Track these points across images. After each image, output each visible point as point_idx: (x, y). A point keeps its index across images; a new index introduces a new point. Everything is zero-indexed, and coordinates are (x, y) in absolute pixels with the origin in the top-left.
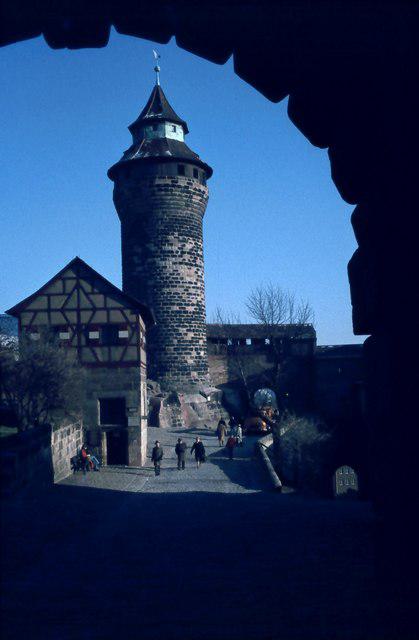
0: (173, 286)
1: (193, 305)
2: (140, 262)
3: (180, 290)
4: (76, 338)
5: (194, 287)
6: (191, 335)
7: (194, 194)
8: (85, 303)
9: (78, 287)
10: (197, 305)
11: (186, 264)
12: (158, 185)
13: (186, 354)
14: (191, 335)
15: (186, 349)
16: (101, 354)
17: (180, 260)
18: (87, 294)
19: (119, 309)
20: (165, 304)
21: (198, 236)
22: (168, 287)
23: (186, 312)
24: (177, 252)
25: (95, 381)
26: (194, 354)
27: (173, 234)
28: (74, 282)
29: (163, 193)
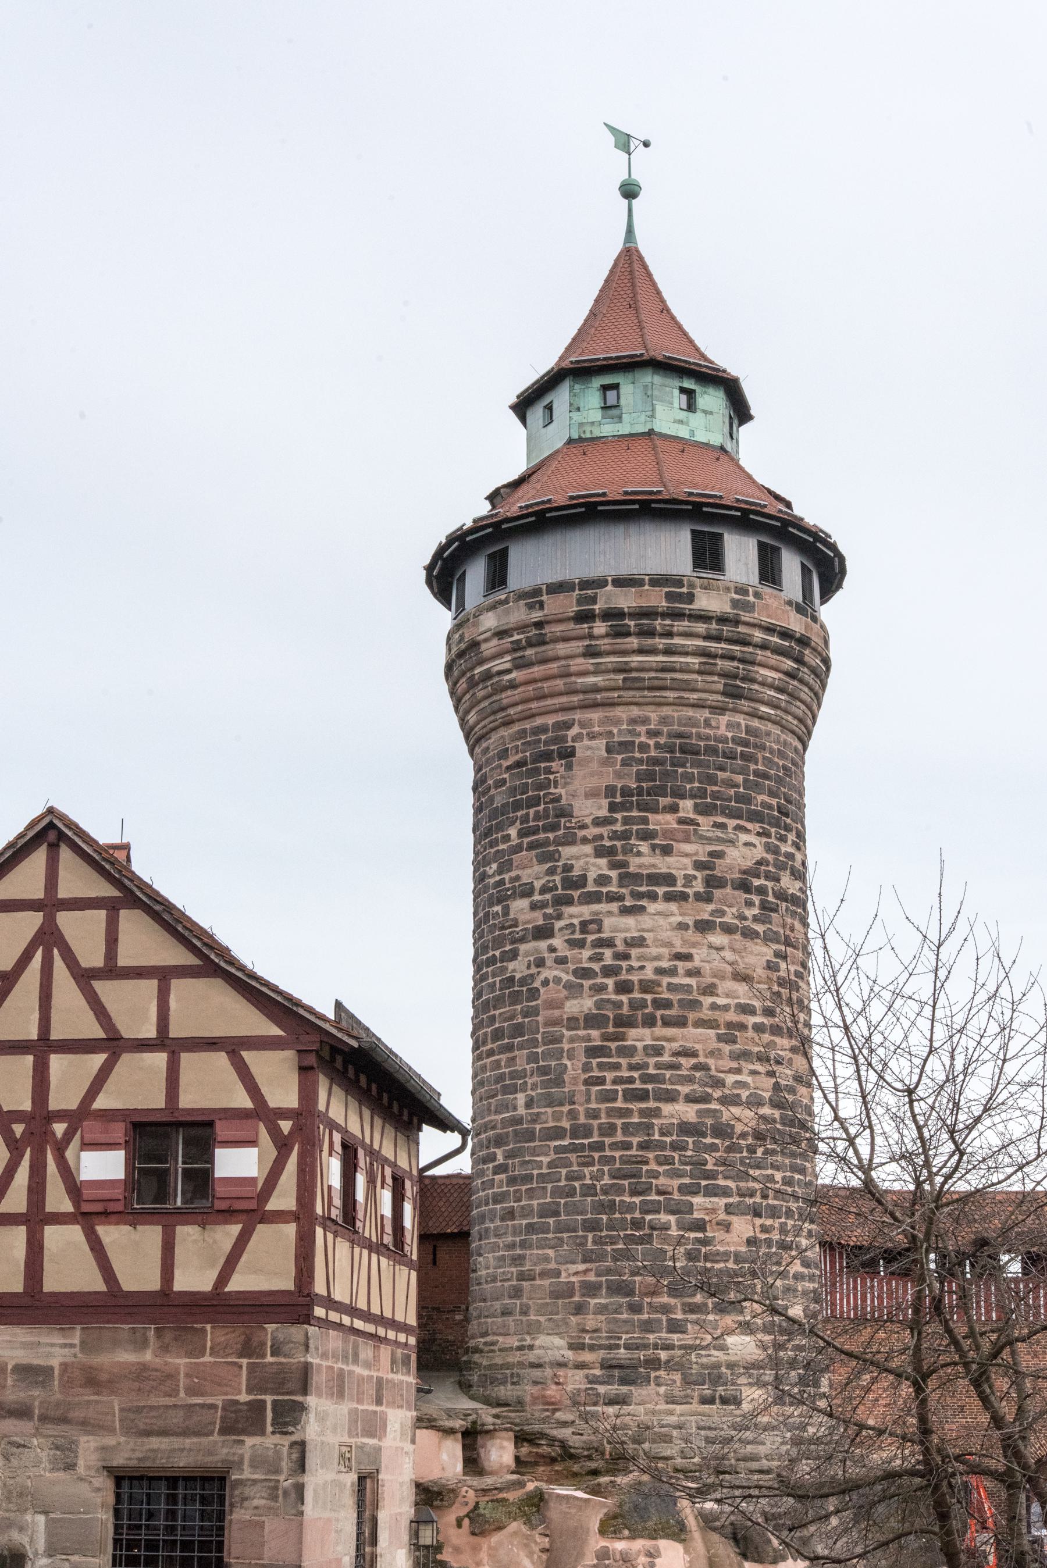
0: (667, 1023)
1: (756, 1102)
2: (538, 918)
3: (698, 1038)
4: (22, 1176)
5: (759, 1028)
6: (743, 1227)
7: (764, 646)
8: (72, 1017)
9: (48, 937)
10: (776, 1105)
11: (728, 929)
12: (612, 615)
14: (743, 1227)
16: (135, 1255)
18: (84, 977)
19: (233, 1047)
20: (643, 1096)
21: (785, 817)
22: (650, 1022)
23: (722, 1131)
24: (689, 880)
25: (92, 1380)
27: (674, 809)
28: (34, 920)
29: (634, 642)
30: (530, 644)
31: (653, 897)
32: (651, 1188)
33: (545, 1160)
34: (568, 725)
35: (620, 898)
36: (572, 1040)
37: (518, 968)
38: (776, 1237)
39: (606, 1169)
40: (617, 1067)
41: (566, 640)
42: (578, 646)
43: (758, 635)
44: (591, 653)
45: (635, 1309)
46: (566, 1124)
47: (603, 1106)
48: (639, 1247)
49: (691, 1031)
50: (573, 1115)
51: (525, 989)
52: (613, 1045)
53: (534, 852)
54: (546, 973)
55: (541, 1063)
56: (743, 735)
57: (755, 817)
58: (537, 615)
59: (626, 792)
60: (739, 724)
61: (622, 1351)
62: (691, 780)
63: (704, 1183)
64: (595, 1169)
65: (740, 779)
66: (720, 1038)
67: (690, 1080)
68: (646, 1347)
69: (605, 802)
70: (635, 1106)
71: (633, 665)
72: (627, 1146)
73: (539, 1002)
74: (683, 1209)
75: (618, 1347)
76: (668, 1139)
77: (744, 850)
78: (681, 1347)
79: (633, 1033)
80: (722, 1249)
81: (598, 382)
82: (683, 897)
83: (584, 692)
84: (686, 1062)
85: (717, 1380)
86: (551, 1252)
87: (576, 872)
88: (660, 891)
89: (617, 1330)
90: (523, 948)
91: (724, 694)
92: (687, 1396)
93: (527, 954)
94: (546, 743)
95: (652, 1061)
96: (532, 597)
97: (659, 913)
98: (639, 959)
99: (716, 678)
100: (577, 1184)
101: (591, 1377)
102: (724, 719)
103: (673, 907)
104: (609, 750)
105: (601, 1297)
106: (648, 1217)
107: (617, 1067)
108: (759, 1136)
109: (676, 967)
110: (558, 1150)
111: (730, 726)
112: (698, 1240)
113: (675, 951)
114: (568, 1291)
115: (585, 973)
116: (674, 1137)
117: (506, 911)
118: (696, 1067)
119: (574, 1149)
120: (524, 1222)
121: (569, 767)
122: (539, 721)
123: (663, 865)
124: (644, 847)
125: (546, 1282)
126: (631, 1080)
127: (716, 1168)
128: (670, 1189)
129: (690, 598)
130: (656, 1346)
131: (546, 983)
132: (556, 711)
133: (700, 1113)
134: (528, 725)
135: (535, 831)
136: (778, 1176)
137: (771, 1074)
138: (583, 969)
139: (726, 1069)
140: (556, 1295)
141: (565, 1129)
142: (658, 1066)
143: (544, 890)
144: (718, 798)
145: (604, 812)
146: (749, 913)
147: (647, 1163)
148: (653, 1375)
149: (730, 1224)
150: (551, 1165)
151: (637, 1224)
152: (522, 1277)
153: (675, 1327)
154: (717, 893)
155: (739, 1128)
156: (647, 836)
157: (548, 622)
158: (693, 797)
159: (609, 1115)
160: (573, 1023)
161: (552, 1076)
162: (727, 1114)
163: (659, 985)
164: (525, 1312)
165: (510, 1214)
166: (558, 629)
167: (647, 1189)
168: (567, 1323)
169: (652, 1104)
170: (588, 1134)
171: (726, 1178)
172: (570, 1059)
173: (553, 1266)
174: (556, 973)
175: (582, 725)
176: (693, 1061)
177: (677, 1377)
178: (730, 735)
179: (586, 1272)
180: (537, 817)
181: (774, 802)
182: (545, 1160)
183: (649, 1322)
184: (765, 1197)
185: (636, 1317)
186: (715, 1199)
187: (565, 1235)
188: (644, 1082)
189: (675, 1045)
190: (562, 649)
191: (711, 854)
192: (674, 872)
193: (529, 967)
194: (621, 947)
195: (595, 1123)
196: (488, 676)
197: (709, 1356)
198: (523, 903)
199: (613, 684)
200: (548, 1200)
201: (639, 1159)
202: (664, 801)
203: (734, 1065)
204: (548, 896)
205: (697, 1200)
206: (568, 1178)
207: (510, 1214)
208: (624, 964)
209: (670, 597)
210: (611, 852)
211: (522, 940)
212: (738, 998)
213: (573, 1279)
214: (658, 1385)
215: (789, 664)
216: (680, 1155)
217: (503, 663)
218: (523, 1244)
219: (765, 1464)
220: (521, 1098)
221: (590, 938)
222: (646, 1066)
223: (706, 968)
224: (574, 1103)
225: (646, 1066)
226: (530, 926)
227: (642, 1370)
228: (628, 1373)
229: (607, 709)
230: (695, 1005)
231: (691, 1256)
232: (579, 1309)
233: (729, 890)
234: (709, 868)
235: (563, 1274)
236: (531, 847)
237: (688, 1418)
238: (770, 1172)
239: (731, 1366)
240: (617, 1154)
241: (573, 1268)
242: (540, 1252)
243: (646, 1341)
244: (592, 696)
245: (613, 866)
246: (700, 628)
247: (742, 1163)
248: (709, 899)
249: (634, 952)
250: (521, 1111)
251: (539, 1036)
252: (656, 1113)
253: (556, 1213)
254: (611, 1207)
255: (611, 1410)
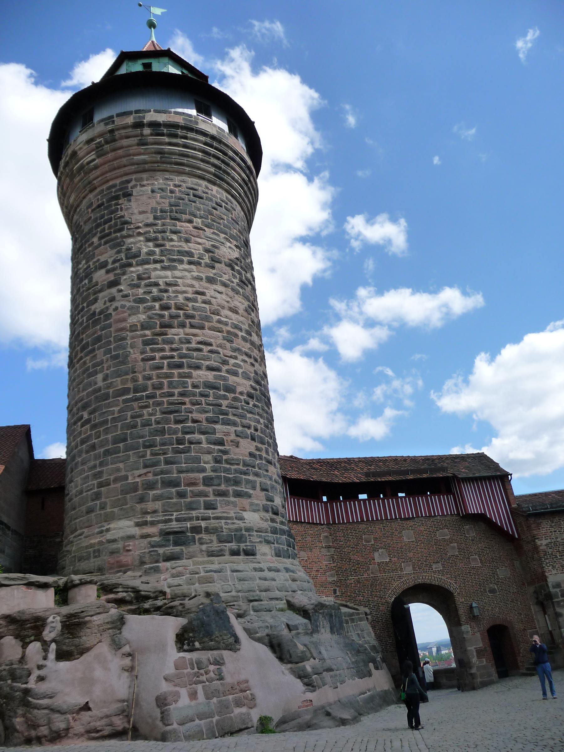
0: (192, 326)
2: (111, 277)
11: (225, 285)
12: (154, 125)
13: (238, 494)
15: (237, 482)
17: (211, 273)
20: (180, 366)
22: (183, 326)
23: (230, 389)
26: (259, 498)
27: (190, 222)
29: (167, 140)
30: (107, 142)
31: (181, 262)
32: (188, 419)
33: (116, 409)
34: (128, 182)
35: (162, 261)
36: (133, 338)
37: (98, 307)
38: (264, 455)
39: (158, 409)
40: (163, 350)
41: (127, 137)
42: (135, 140)
43: (231, 153)
44: (142, 143)
45: (181, 495)
46: (130, 385)
47: (154, 373)
48: (183, 455)
49: (207, 331)
50: (135, 380)
51: (102, 316)
52: (160, 338)
53: (108, 245)
54: (115, 304)
55: (113, 353)
56: (225, 199)
57: (232, 237)
58: (110, 127)
59: (162, 211)
60: (222, 194)
61: (174, 523)
62: (199, 209)
63: (221, 417)
64: (150, 409)
65: (225, 217)
66: (224, 338)
67: (208, 359)
68: (191, 519)
69: (151, 216)
70: (175, 372)
71: (166, 150)
72: (172, 395)
73: (112, 320)
74: (210, 431)
75: (170, 520)
76: (197, 390)
77: (229, 251)
78: (215, 518)
79: (173, 331)
80: (235, 457)
81: (141, 62)
82: (199, 264)
83: (137, 164)
84: (206, 348)
85: (240, 539)
86: (121, 465)
87: (134, 250)
88: (186, 259)
89: (170, 510)
90: (101, 295)
91: (215, 175)
92: (221, 550)
93: (104, 297)
94: (115, 192)
95: (185, 346)
96: (109, 120)
97: (185, 270)
98: (174, 292)
99: (210, 166)
100: (138, 420)
101: (152, 543)
102: (215, 188)
103: (193, 267)
104: (153, 191)
105: (157, 489)
106: (187, 437)
107: (163, 350)
108: (251, 396)
109: (197, 297)
110: (125, 401)
111: (217, 191)
112: (221, 451)
113: (195, 289)
114: (134, 488)
115: (142, 301)
116: (201, 389)
117: (91, 280)
118: (211, 352)
119: (136, 399)
120: (102, 450)
121: (130, 201)
122: (111, 183)
123: (186, 247)
124: (175, 237)
125: (118, 485)
126: (172, 357)
127: (227, 409)
128: (201, 419)
129: (197, 123)
130: (198, 519)
131: (116, 309)
132: (122, 176)
133: (216, 377)
134: (104, 187)
135: (109, 234)
136: (262, 421)
137: (253, 365)
138: (140, 298)
139: (229, 355)
140: (125, 492)
141: (130, 388)
142: (189, 349)
143: (114, 262)
144: (214, 221)
145: (151, 220)
146: (234, 280)
147: (184, 404)
148: (197, 537)
149: (238, 442)
150: (119, 412)
151: (180, 442)
152: (100, 485)
153: (210, 506)
154: (217, 265)
155: (239, 389)
156: (175, 232)
157: (118, 129)
158: (201, 217)
159: (158, 377)
160: (133, 328)
161: (121, 359)
162: (232, 379)
163: (187, 306)
164: (102, 508)
165: (93, 447)
166: (123, 132)
167: (186, 419)
168: (133, 510)
169: (186, 370)
170: (145, 389)
171: (234, 415)
172: (132, 348)
173: (123, 473)
174: (123, 303)
175: (136, 180)
176: (210, 348)
177: (214, 538)
178: (218, 196)
179: (145, 474)
180: (110, 227)
181: (242, 237)
182: (116, 409)
183: (191, 503)
184: (256, 430)
185: (182, 500)
186: (229, 427)
187: (131, 453)
188: (181, 357)
189: (199, 339)
190: (125, 142)
191: (213, 246)
192: (193, 250)
193: (105, 303)
194: (162, 287)
195: (149, 383)
196: (82, 167)
197: (234, 523)
198: (103, 271)
199: (154, 159)
200: (119, 432)
201: (180, 401)
202: (184, 217)
203: (234, 354)
204: (117, 264)
205: (218, 427)
206: (132, 417)
207: (93, 447)
208: (165, 295)
209: (184, 119)
210: (156, 239)
211: (101, 291)
212: (232, 320)
213: (138, 480)
214: (201, 544)
215: (244, 175)
216: (205, 400)
217: (92, 156)
218: (101, 464)
219: (277, 594)
220: (100, 377)
221: (143, 283)
222: (181, 349)
223: (213, 301)
224: (135, 372)
225: (181, 349)
226: (106, 282)
227: (189, 534)
228: (178, 537)
229: (151, 173)
230: (207, 319)
231: (217, 461)
232: (142, 500)
233: (223, 265)
234: (212, 252)
235: (130, 478)
236: (106, 243)
237: (223, 565)
238: (257, 417)
239: (248, 530)
240: (165, 400)
241: (137, 473)
242: (114, 466)
243: (190, 515)
244: (143, 166)
245: (157, 246)
246: (203, 138)
247: (243, 409)
248: (213, 268)
249: (170, 289)
250: (100, 384)
251: (112, 339)
252: (189, 376)
253: (125, 440)
254: (162, 432)
255: (168, 564)
